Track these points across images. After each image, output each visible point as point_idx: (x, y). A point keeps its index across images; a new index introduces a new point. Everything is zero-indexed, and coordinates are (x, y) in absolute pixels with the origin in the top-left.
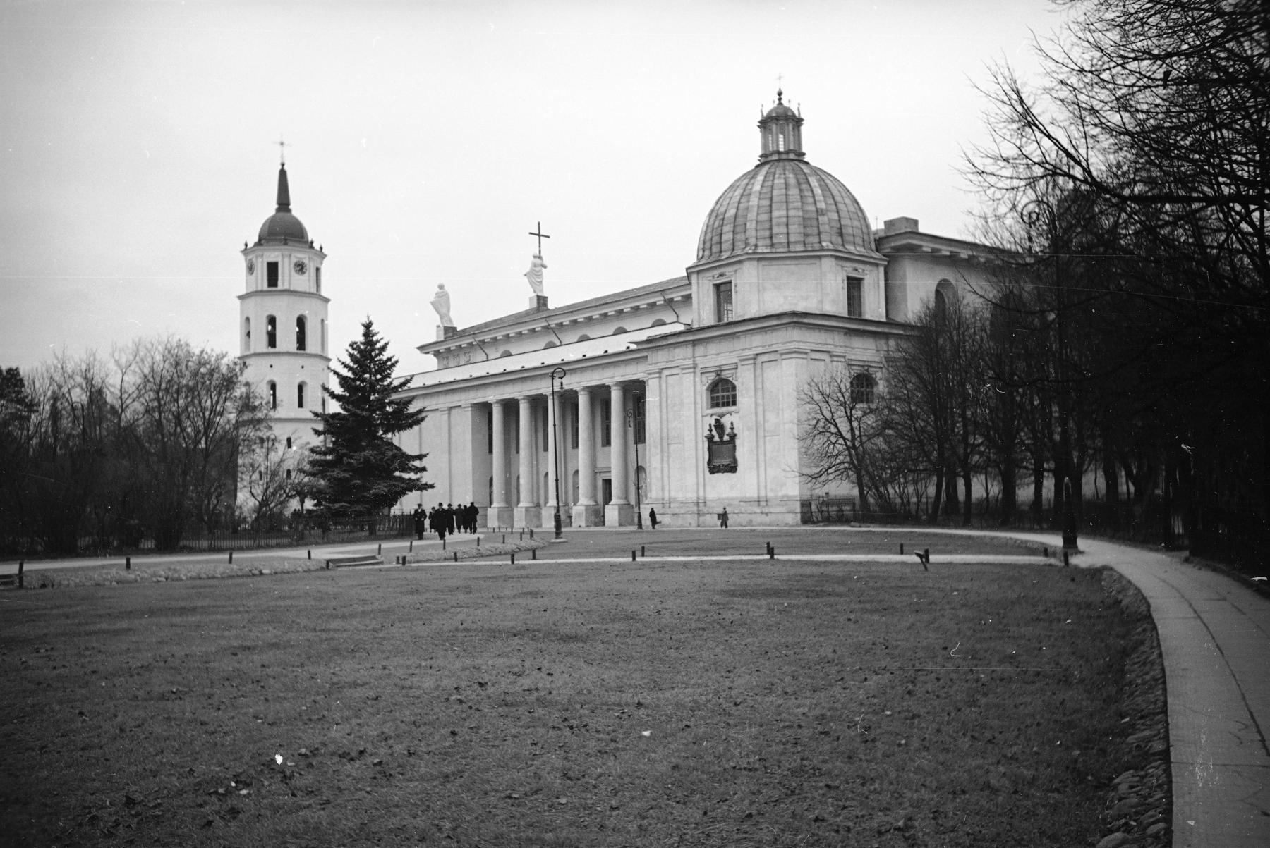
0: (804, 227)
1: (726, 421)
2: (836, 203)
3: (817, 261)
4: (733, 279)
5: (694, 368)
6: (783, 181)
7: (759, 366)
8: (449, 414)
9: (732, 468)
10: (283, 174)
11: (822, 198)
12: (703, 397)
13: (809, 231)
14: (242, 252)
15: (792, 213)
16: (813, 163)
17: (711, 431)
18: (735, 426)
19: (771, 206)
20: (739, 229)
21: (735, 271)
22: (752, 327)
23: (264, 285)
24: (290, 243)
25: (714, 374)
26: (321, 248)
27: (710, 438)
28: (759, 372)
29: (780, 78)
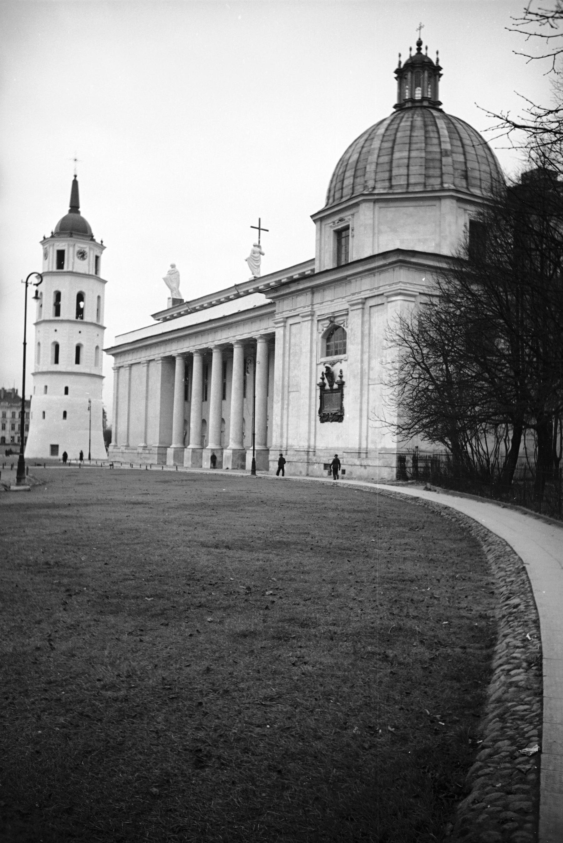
0: (426, 168)
1: (336, 369)
2: (463, 146)
3: (437, 203)
4: (350, 223)
5: (312, 315)
6: (409, 123)
7: (367, 311)
8: (148, 366)
9: (339, 417)
10: (75, 183)
11: (448, 139)
12: (319, 344)
13: (431, 172)
14: (41, 242)
15: (413, 154)
16: (447, 111)
17: (323, 379)
18: (344, 374)
19: (393, 148)
20: (359, 173)
21: (353, 215)
22: (360, 269)
23: (55, 269)
24: (74, 236)
25: (327, 322)
26: (102, 242)
27: (322, 386)
28: (366, 317)
29: (420, 28)
